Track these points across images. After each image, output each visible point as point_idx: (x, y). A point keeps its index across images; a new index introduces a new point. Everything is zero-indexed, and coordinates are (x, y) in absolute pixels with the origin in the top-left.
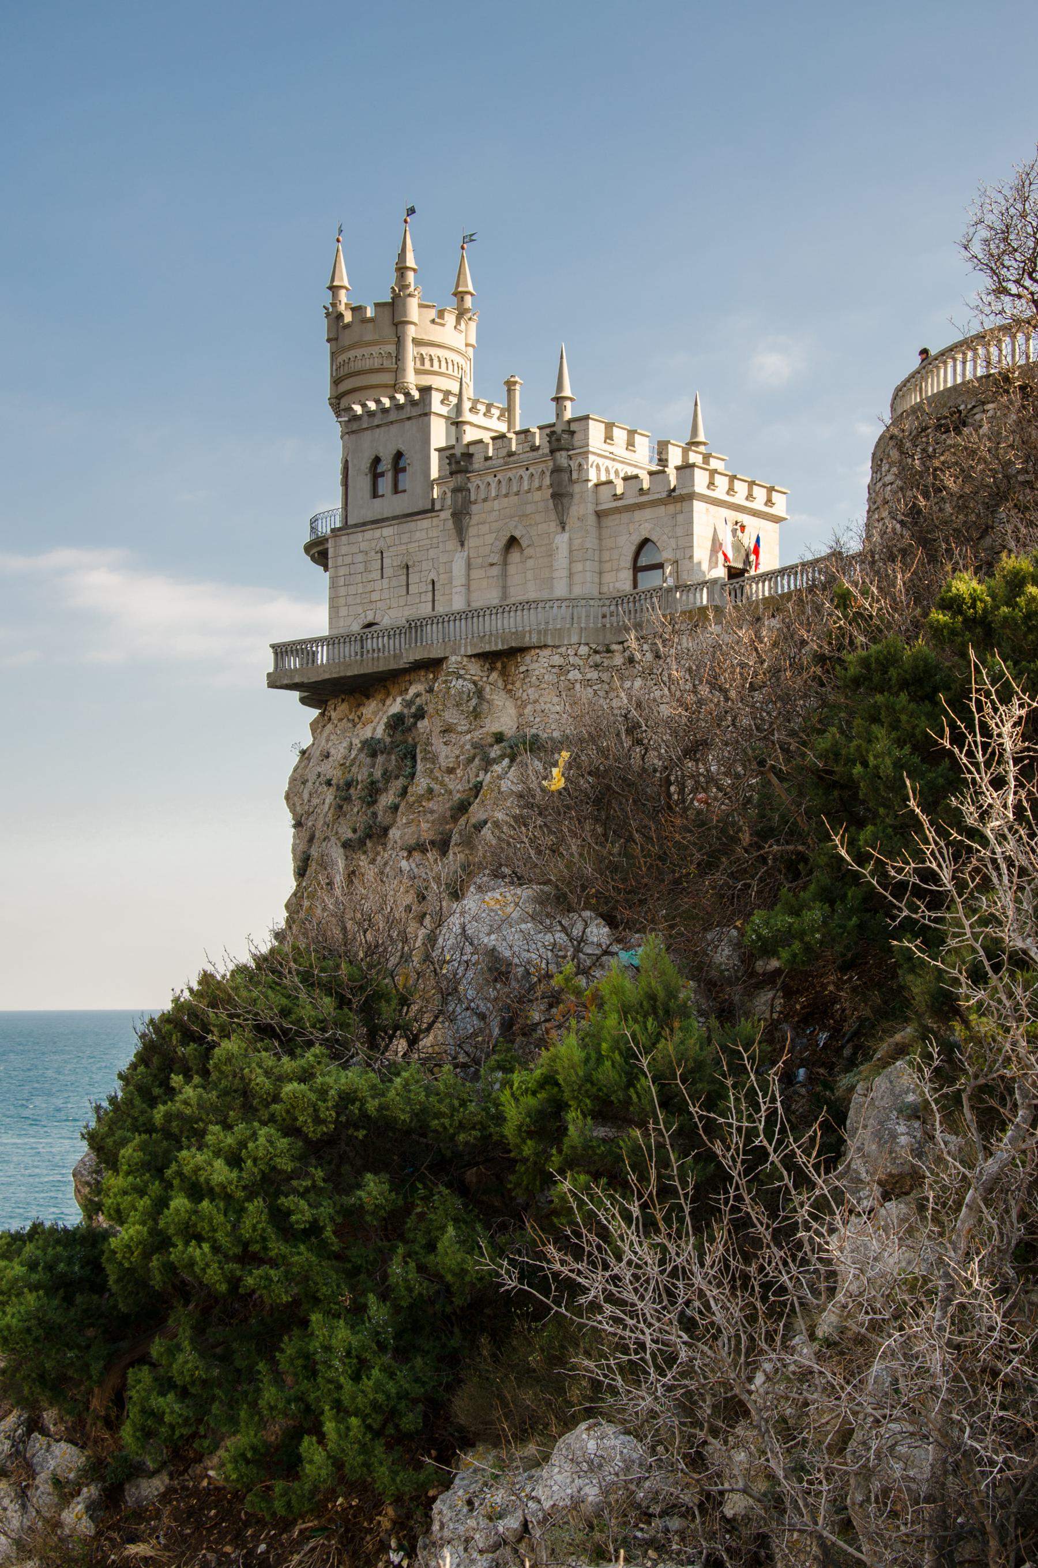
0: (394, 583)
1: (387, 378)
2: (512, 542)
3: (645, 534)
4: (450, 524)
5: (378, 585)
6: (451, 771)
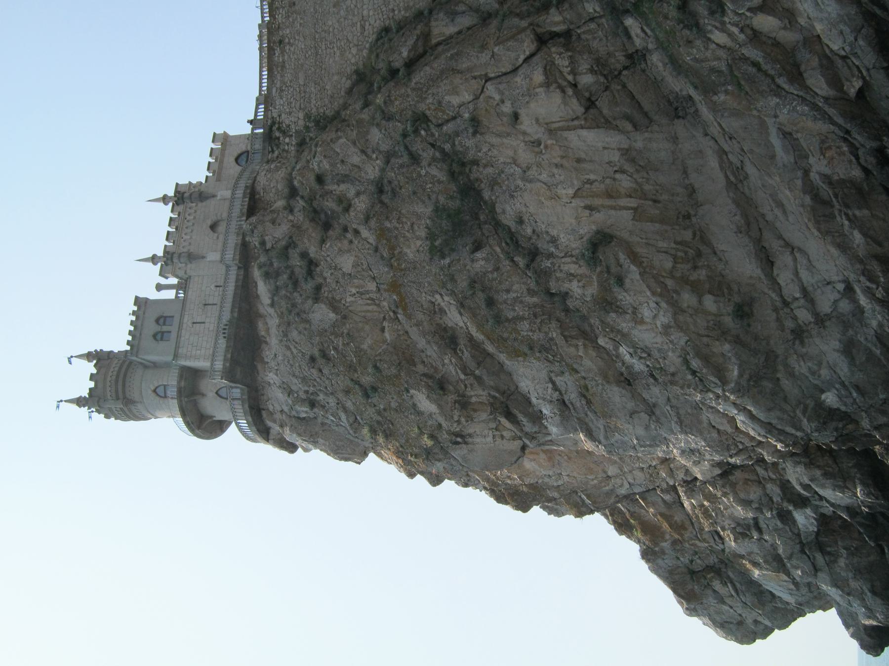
3: (232, 159)
5: (207, 325)
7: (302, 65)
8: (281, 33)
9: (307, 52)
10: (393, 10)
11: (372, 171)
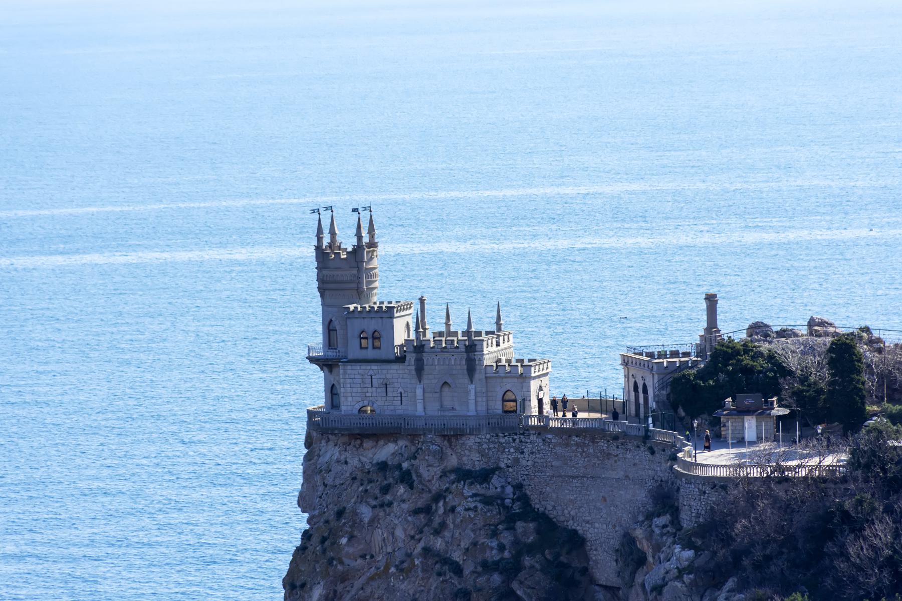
0: (379, 390)
1: (354, 285)
2: (445, 383)
4: (414, 372)
5: (370, 390)
6: (429, 481)
7: (567, 464)
8: (591, 444)
9: (576, 468)
10: (596, 550)
11: (457, 556)
